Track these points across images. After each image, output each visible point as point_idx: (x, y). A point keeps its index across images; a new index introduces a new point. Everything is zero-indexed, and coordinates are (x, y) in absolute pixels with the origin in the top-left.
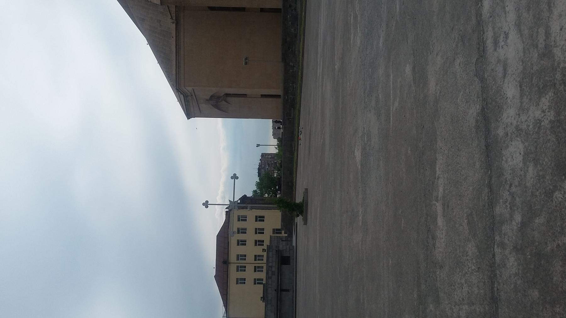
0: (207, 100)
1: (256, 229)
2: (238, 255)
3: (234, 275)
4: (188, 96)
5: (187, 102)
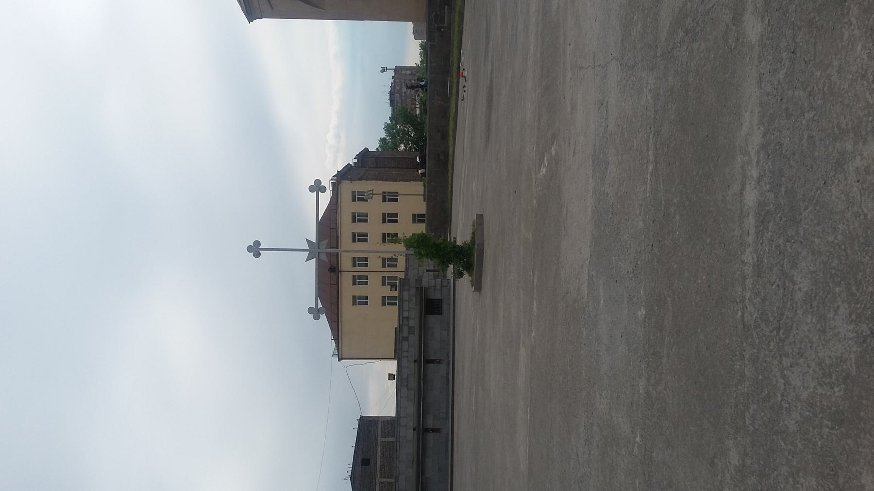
1: (384, 214)
3: (348, 290)
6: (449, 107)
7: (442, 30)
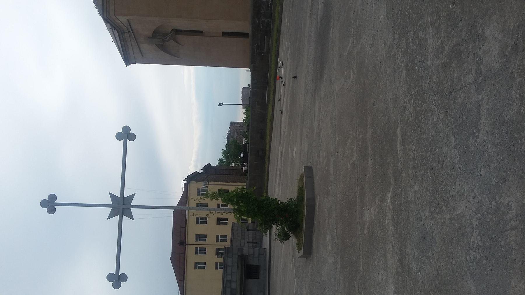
0: (149, 38)
2: (197, 236)
3: (192, 258)
4: (124, 32)
5: (124, 42)
6: (267, 113)
7: (262, 54)
